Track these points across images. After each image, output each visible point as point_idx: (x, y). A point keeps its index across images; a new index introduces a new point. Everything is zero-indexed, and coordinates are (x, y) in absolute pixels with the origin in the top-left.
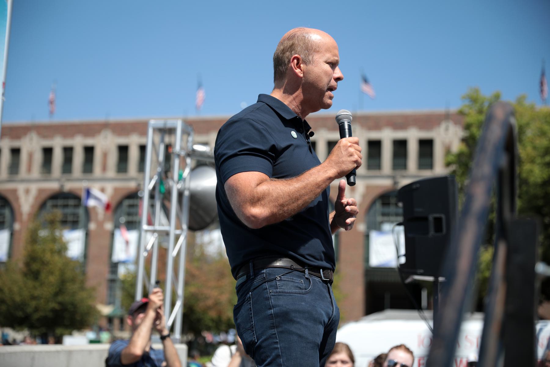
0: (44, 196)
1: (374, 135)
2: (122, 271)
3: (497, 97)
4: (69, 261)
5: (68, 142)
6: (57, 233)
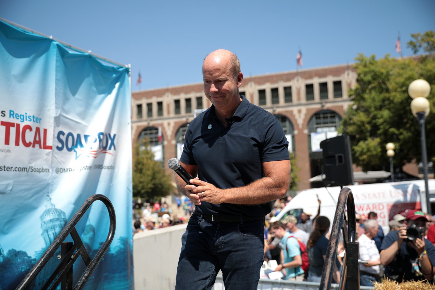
0: (140, 129)
1: (309, 82)
3: (373, 58)
4: (156, 162)
5: (149, 101)
6: (149, 148)
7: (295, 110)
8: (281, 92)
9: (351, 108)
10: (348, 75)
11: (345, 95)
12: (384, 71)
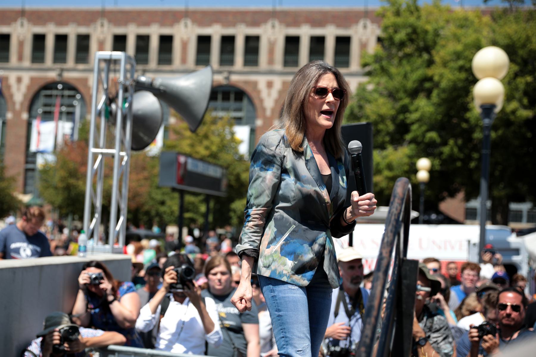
1: (293, 32)
2: (40, 161)
7: (262, 81)
8: (240, 45)
9: (362, 88)
10: (365, 27)
11: (355, 65)
12: (429, 27)
